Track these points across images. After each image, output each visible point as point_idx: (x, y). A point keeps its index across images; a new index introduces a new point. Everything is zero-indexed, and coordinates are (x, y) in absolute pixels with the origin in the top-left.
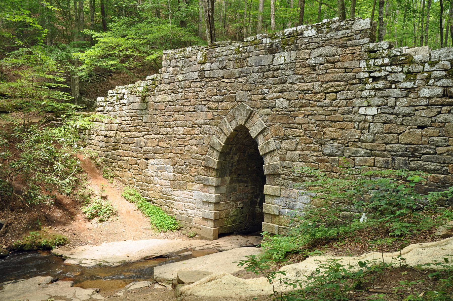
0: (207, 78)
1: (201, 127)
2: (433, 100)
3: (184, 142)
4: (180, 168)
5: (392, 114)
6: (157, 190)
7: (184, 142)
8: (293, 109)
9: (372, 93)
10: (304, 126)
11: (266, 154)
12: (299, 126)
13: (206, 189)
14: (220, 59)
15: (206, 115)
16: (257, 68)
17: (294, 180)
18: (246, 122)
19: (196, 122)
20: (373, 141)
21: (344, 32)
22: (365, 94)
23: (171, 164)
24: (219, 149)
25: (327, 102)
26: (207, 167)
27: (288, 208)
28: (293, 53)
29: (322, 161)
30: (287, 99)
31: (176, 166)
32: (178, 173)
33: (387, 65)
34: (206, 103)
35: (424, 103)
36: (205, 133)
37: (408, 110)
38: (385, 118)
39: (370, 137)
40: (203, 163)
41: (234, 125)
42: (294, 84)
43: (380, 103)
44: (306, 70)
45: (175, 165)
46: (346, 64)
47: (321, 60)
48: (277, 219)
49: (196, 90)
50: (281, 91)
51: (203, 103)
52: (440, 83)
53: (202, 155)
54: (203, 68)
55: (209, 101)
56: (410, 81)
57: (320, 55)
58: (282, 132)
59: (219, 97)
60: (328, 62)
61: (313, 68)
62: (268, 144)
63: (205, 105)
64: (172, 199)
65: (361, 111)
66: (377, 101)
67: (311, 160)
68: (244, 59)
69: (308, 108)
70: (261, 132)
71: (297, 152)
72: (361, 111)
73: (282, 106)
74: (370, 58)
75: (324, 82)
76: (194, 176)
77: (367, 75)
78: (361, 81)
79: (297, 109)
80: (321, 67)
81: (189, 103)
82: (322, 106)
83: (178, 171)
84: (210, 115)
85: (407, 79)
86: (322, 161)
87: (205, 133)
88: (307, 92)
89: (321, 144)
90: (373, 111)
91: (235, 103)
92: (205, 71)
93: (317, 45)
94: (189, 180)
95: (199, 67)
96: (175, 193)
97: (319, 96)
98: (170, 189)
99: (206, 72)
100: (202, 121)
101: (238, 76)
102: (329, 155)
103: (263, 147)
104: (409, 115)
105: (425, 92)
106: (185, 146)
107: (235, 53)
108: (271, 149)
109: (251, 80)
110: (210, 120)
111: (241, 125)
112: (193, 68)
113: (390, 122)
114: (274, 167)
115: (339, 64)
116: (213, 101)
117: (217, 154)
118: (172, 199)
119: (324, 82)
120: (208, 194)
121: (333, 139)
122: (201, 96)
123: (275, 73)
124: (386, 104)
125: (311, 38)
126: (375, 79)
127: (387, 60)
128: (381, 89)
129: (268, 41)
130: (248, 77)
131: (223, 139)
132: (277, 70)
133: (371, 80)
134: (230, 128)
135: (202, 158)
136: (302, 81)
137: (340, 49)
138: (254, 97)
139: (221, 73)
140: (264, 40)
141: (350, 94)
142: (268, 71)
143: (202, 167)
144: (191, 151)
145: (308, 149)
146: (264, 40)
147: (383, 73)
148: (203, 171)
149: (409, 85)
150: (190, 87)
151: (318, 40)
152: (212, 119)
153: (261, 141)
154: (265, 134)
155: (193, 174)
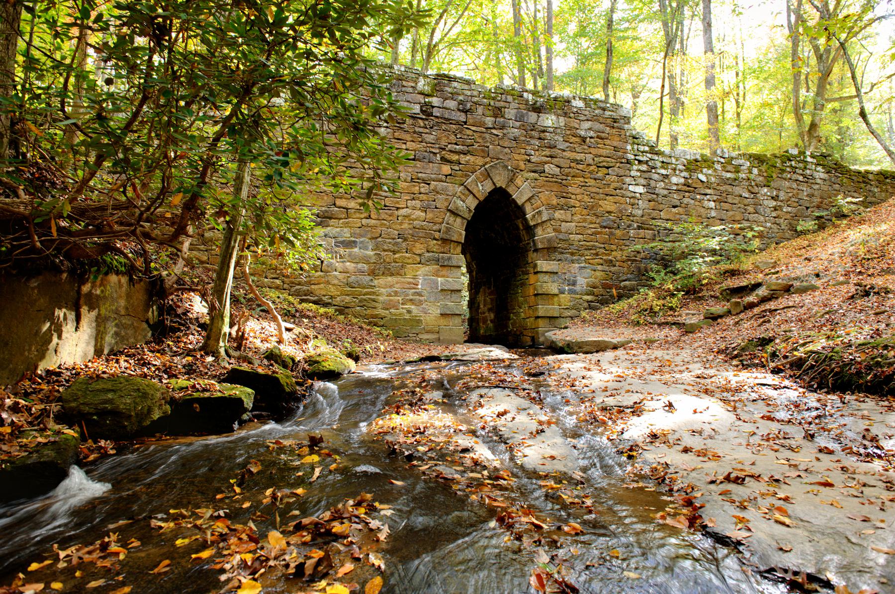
0: (437, 117)
1: (429, 184)
2: (680, 187)
3: (398, 203)
4: (390, 243)
5: (654, 194)
6: (336, 282)
7: (398, 203)
8: (565, 177)
9: (639, 174)
10: (579, 197)
11: (535, 226)
12: (573, 196)
13: (444, 272)
14: (461, 98)
15: (440, 169)
16: (518, 124)
17: (572, 254)
18: (508, 186)
19: (420, 175)
20: (642, 216)
21: (610, 113)
22: (633, 173)
23: (369, 236)
24: (468, 216)
25: (600, 175)
26: (445, 241)
27: (569, 285)
28: (562, 119)
29: (599, 233)
30: (558, 167)
31: (380, 239)
32: (385, 250)
33: (646, 152)
34: (437, 151)
35: (675, 188)
36: (438, 193)
37: (666, 192)
38: (650, 197)
39: (640, 212)
40: (437, 235)
41: (488, 187)
42: (564, 151)
43: (645, 183)
44: (577, 140)
45: (376, 238)
46: (615, 144)
47: (592, 134)
48: (556, 299)
49: (417, 129)
50: (551, 157)
51: (434, 150)
52: (683, 174)
53: (435, 223)
54: (429, 102)
55: (444, 149)
56: (665, 169)
57: (590, 129)
58: (555, 201)
59: (462, 147)
60: (598, 137)
61: (584, 140)
62: (540, 213)
63: (435, 154)
64: (374, 293)
65: (631, 188)
66: (643, 181)
67: (589, 232)
68: (499, 109)
69: (582, 179)
70: (529, 199)
71: (573, 224)
72: (631, 188)
73: (551, 172)
74: (634, 143)
75: (596, 156)
76: (420, 255)
77: (633, 157)
78: (628, 162)
79: (569, 178)
80: (592, 140)
81: (404, 147)
82: (595, 179)
83: (386, 248)
84: (446, 169)
85: (662, 167)
86: (599, 233)
87: (438, 193)
88: (578, 162)
89: (597, 216)
90: (640, 189)
91: (488, 159)
92: (433, 107)
93: (585, 118)
94: (410, 261)
95: (421, 99)
96: (376, 282)
97: (592, 168)
98: (368, 278)
99: (435, 109)
100: (433, 176)
101: (490, 126)
102: (605, 227)
103: (534, 216)
104: (665, 196)
105: (674, 180)
106: (398, 209)
107: (484, 97)
108: (544, 219)
109: (511, 136)
110: (446, 176)
111: (501, 187)
112: (409, 97)
113: (654, 200)
114: (549, 240)
115: (607, 142)
116: (451, 151)
117: (463, 224)
118: (374, 293)
119: (596, 156)
120: (450, 280)
121: (608, 212)
122: (428, 140)
123: (542, 135)
124: (649, 185)
125: (580, 109)
126: (640, 162)
127: (647, 149)
128: (644, 172)
129: (530, 97)
130: (505, 131)
131: (472, 203)
132: (544, 131)
133: (636, 162)
134: (483, 189)
135: (434, 228)
136: (573, 150)
137: (608, 128)
138: (517, 157)
139: (462, 117)
140: (525, 95)
141: (621, 172)
142: (532, 130)
143: (435, 242)
144: (413, 217)
145: (585, 221)
146: (525, 95)
147: (645, 159)
148: (437, 247)
149: (663, 172)
150: (404, 123)
151: (587, 113)
152: (450, 175)
153: (528, 208)
154: (533, 201)
155: (418, 252)
